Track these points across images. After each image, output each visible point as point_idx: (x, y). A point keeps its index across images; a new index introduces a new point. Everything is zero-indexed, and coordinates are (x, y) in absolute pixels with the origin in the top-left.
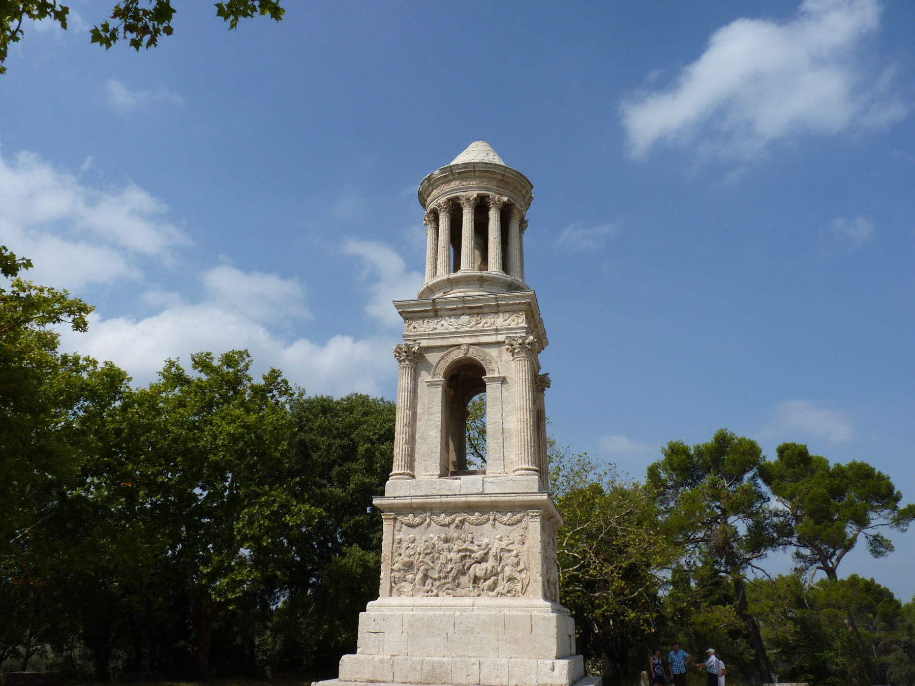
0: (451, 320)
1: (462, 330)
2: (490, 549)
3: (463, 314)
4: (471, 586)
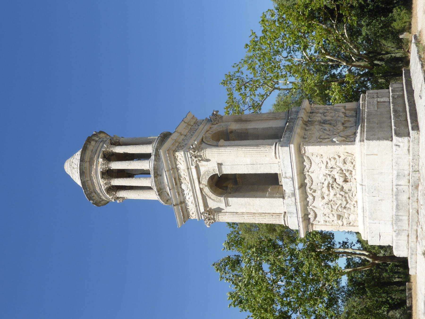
0: (185, 194)
1: (190, 188)
2: (327, 174)
3: (181, 188)
4: (350, 183)
